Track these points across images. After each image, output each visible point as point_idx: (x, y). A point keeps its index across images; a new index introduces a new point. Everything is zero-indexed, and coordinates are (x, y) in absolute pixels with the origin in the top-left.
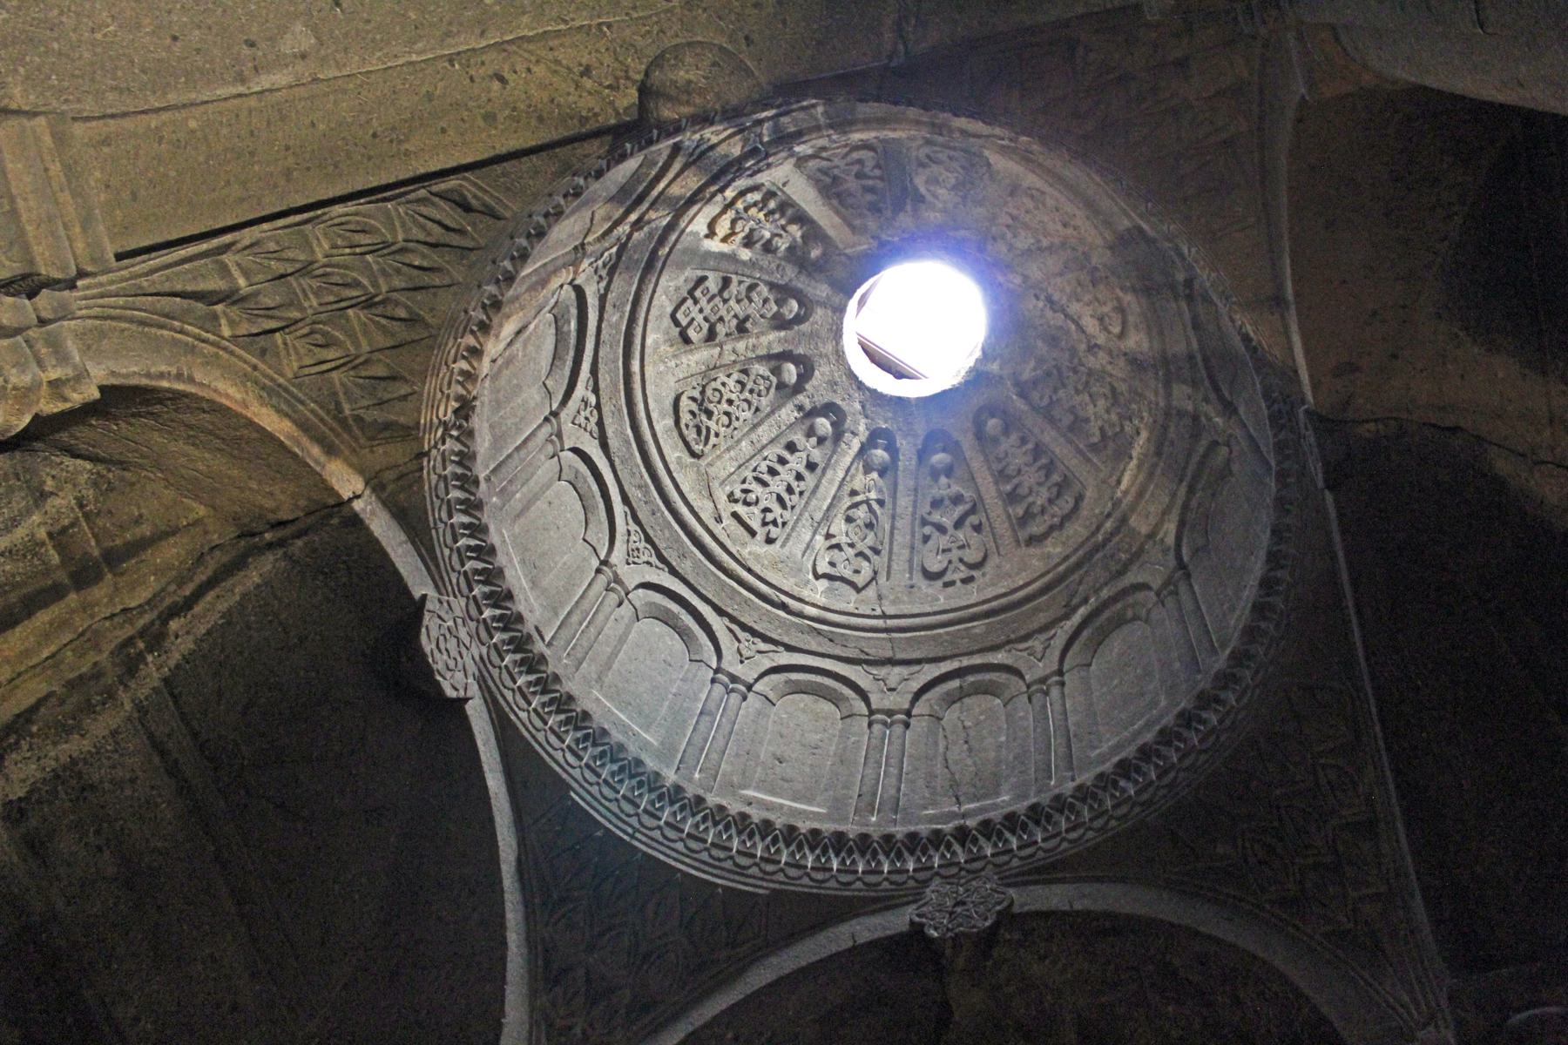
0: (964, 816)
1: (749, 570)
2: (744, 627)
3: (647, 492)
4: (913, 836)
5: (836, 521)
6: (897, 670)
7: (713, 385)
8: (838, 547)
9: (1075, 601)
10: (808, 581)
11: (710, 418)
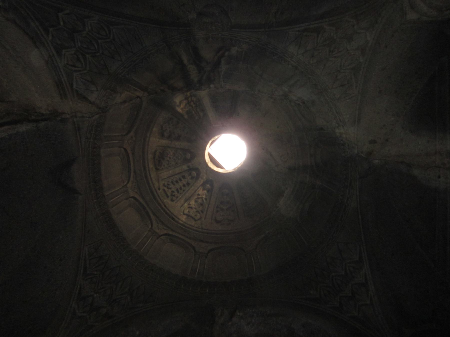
1: (165, 206)
8: (191, 208)
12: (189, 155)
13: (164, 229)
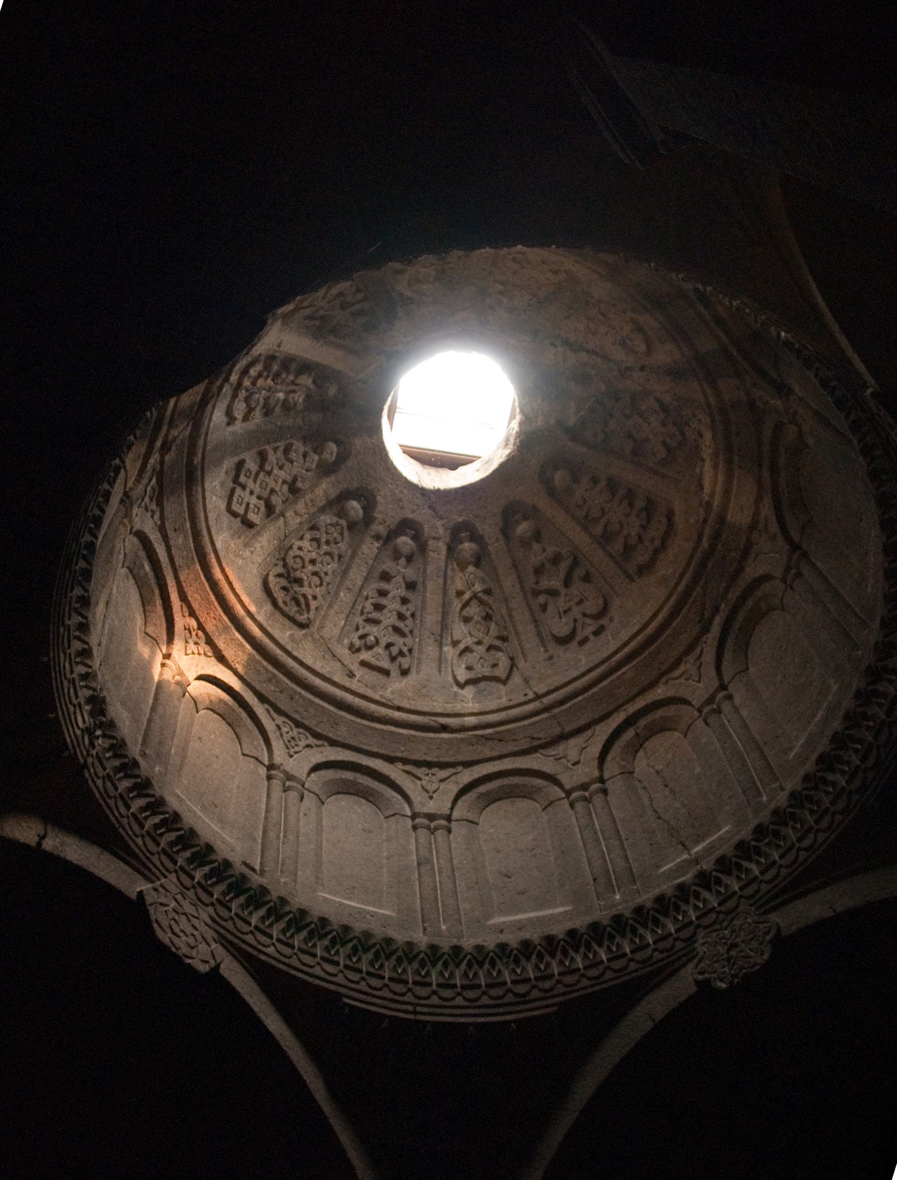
0: (697, 861)
1: (399, 709)
2: (418, 764)
3: (278, 682)
4: (660, 899)
5: (456, 626)
6: (572, 742)
7: (291, 553)
9: (707, 614)
10: (456, 694)
11: (302, 586)
12: (355, 504)
13: (442, 781)
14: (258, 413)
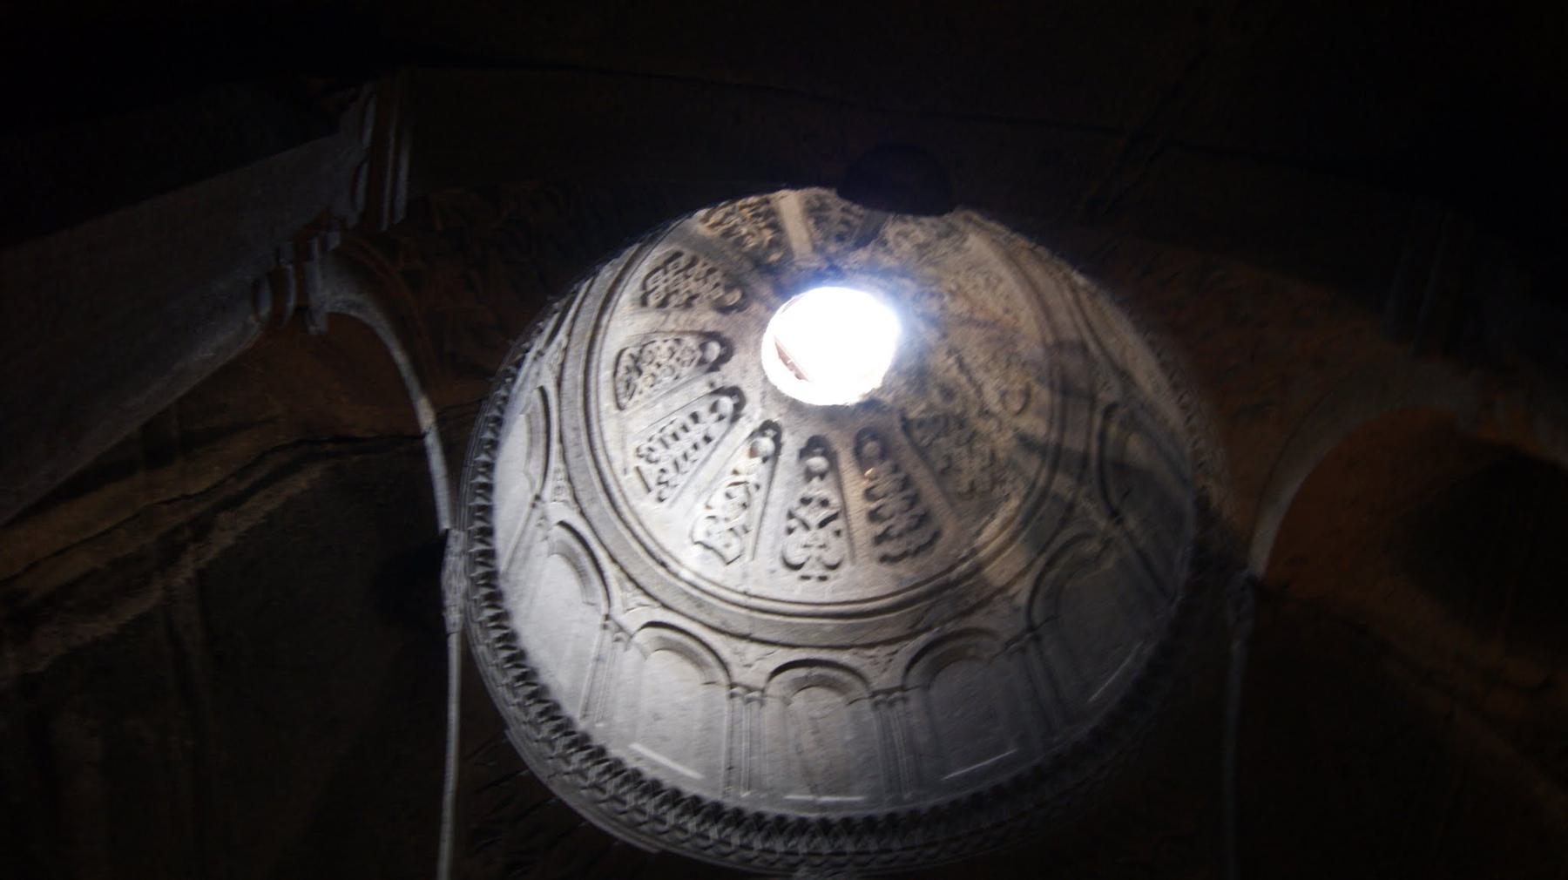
1: (641, 524)
2: (631, 579)
3: (578, 436)
9: (920, 626)
14: (721, 229)
